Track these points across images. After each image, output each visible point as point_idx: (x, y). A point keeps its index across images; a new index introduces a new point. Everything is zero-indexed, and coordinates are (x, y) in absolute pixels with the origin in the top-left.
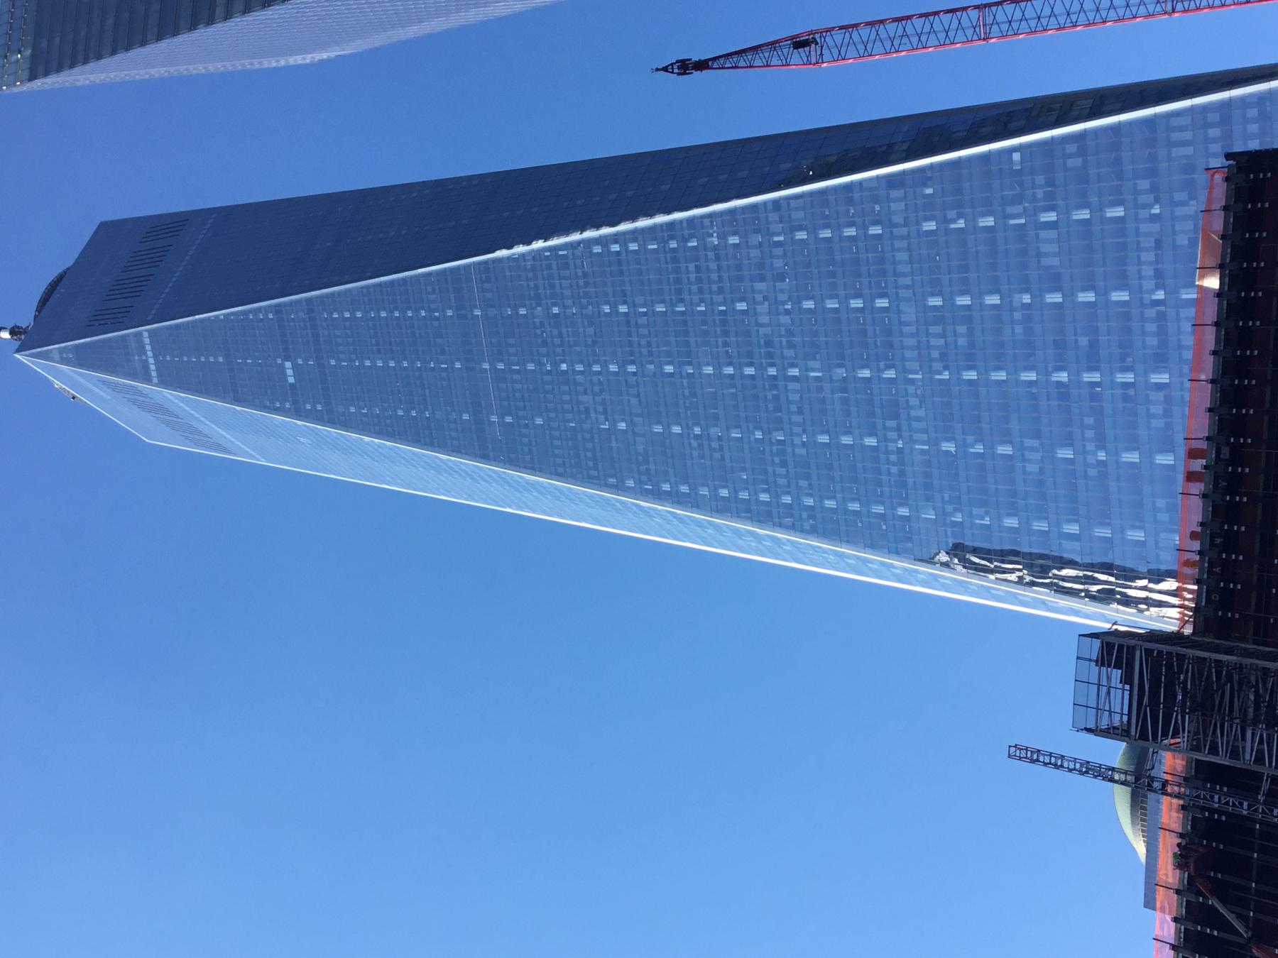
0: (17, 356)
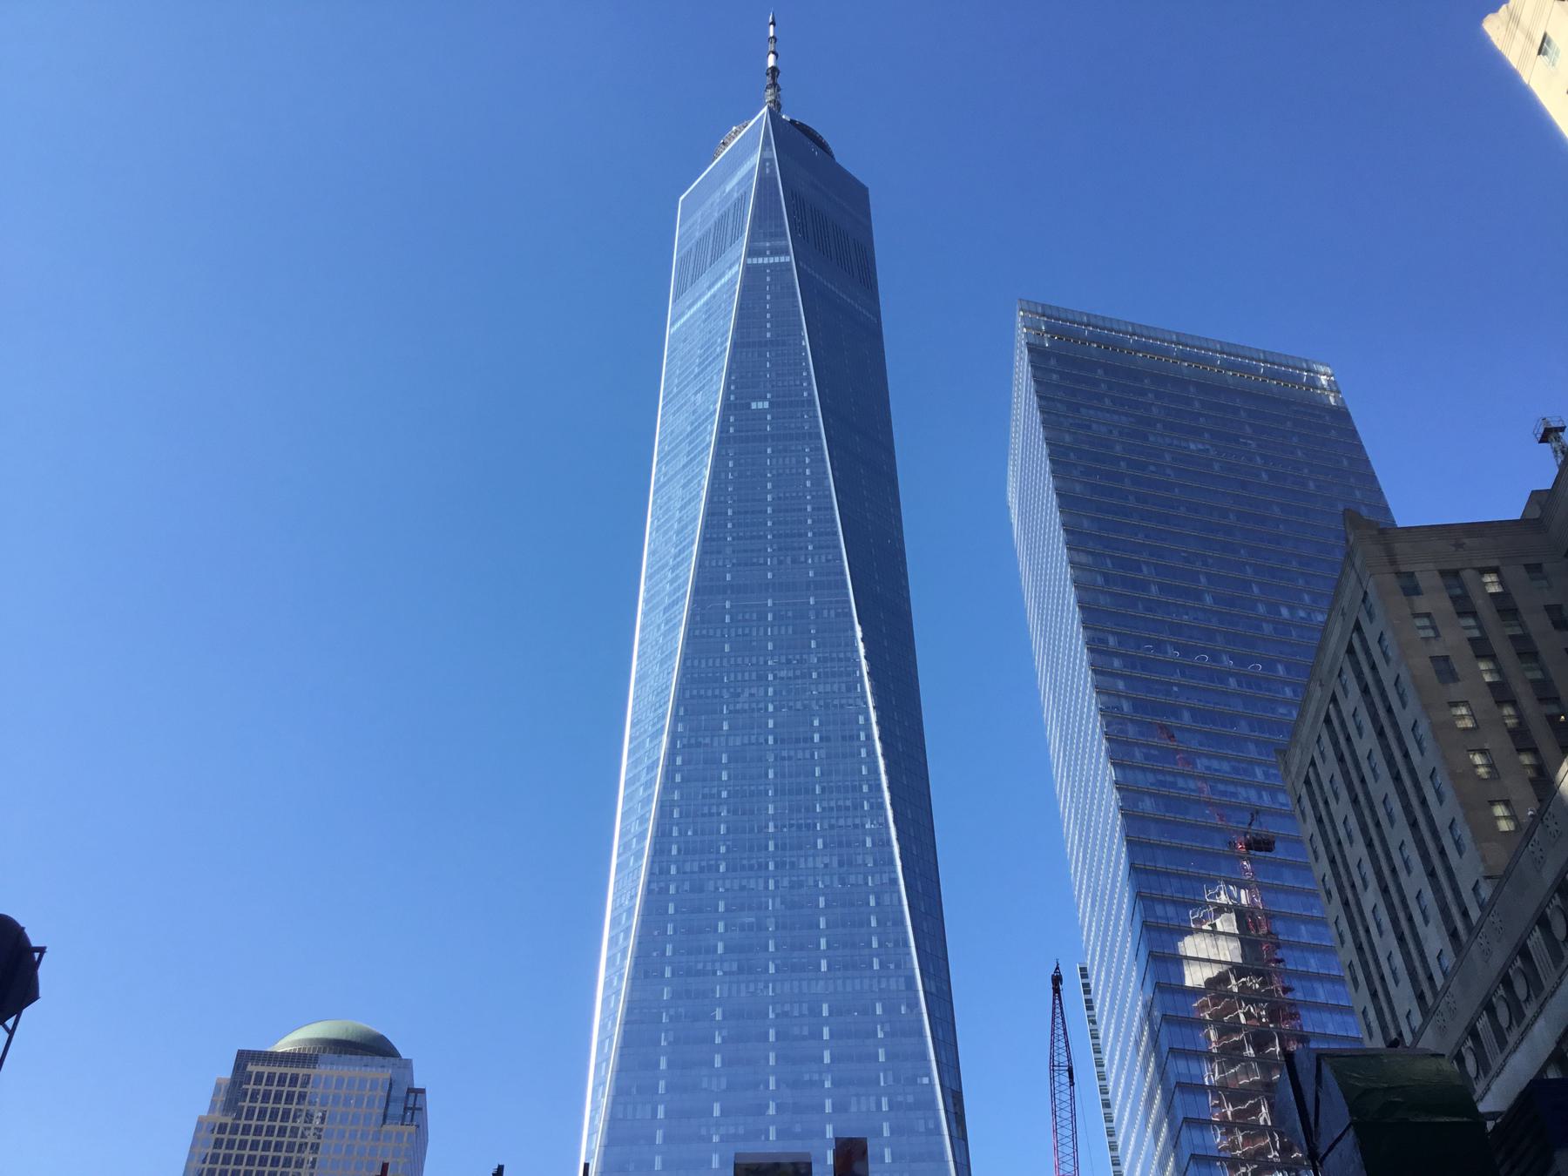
0: (765, 109)
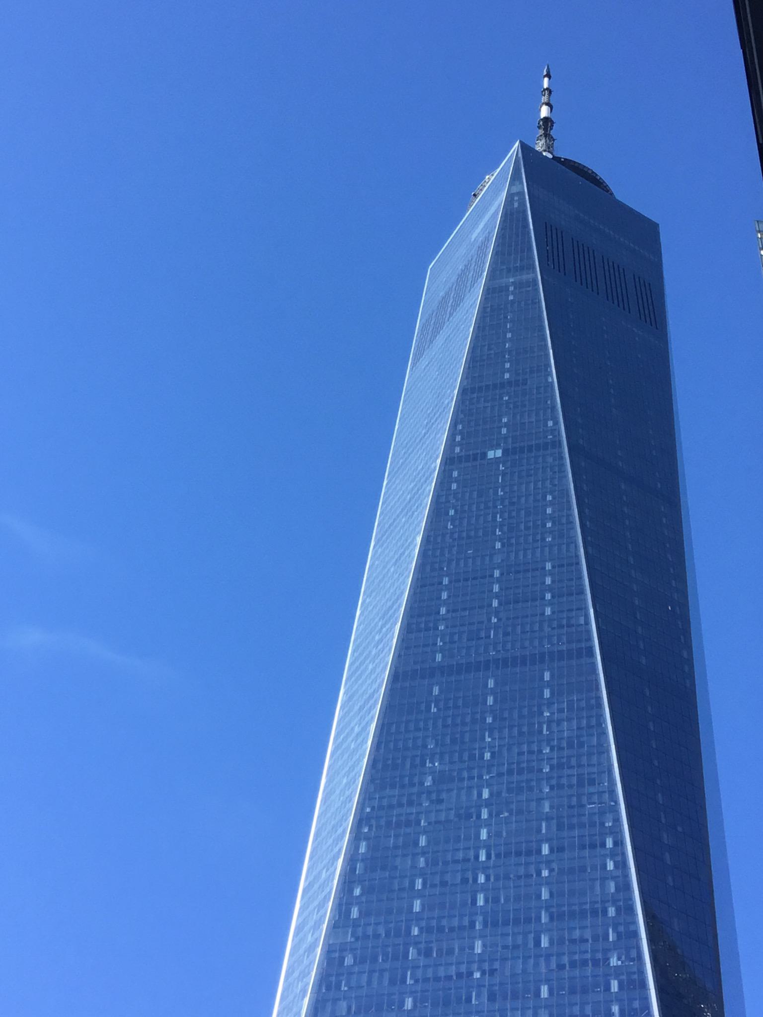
0: (517, 144)
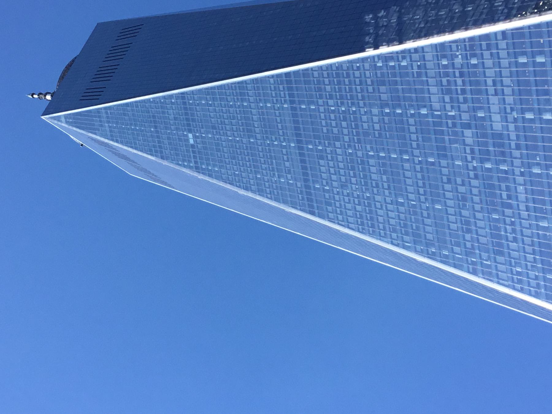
0: (43, 117)
